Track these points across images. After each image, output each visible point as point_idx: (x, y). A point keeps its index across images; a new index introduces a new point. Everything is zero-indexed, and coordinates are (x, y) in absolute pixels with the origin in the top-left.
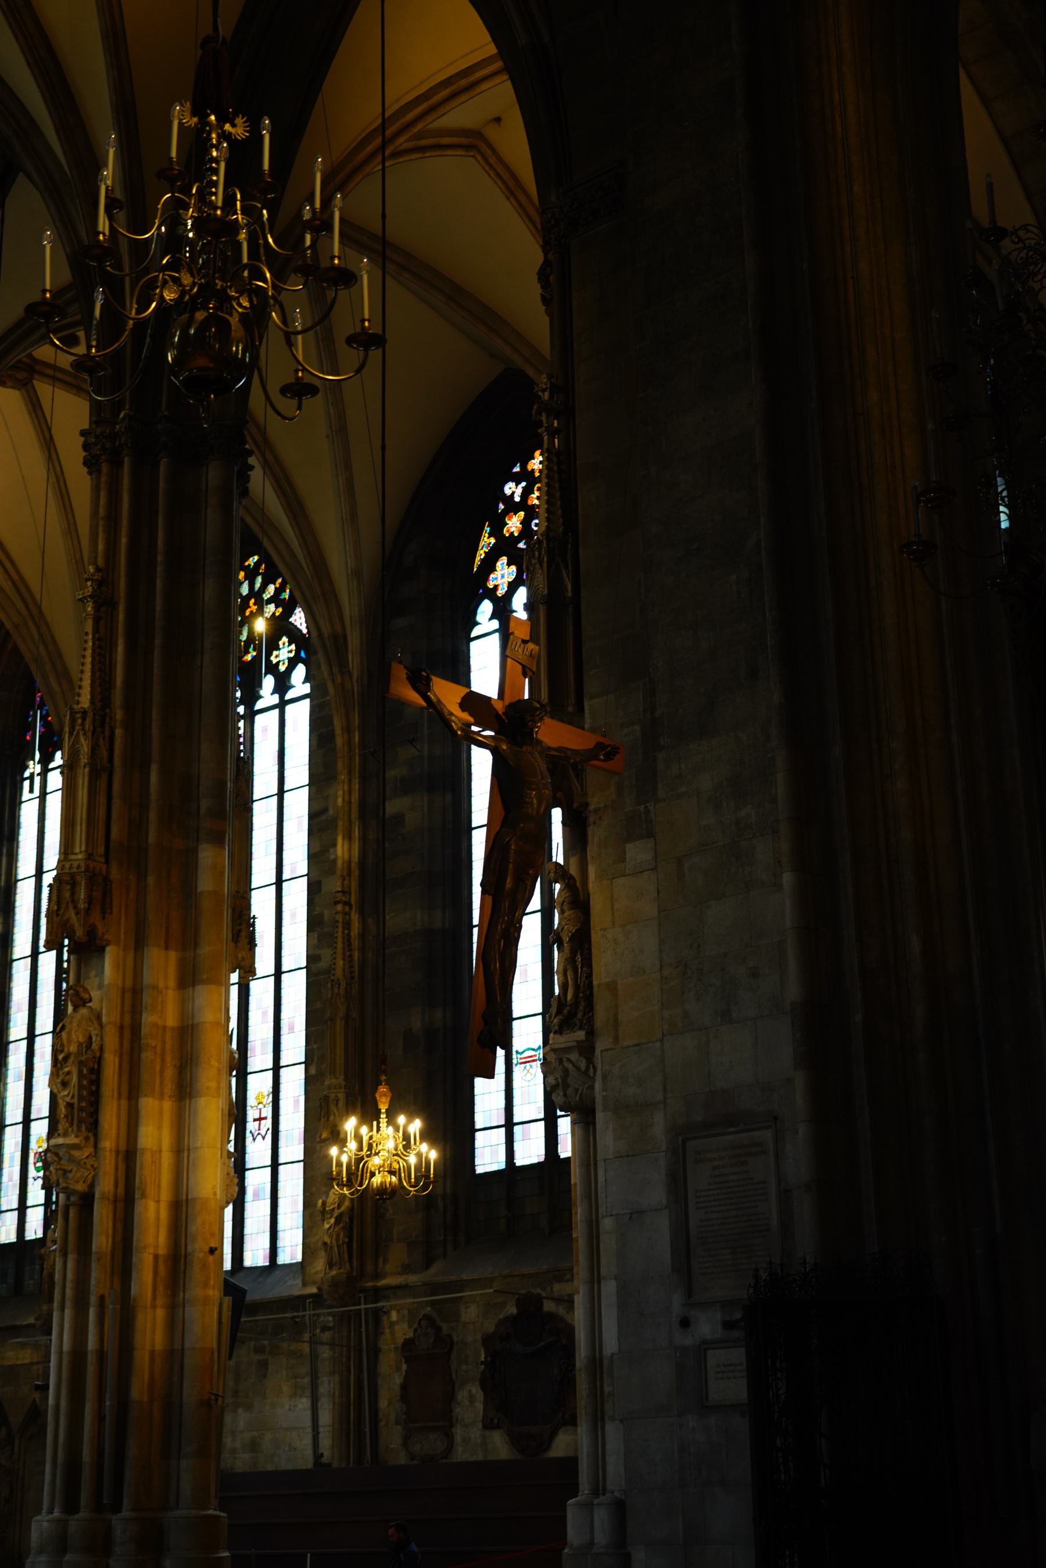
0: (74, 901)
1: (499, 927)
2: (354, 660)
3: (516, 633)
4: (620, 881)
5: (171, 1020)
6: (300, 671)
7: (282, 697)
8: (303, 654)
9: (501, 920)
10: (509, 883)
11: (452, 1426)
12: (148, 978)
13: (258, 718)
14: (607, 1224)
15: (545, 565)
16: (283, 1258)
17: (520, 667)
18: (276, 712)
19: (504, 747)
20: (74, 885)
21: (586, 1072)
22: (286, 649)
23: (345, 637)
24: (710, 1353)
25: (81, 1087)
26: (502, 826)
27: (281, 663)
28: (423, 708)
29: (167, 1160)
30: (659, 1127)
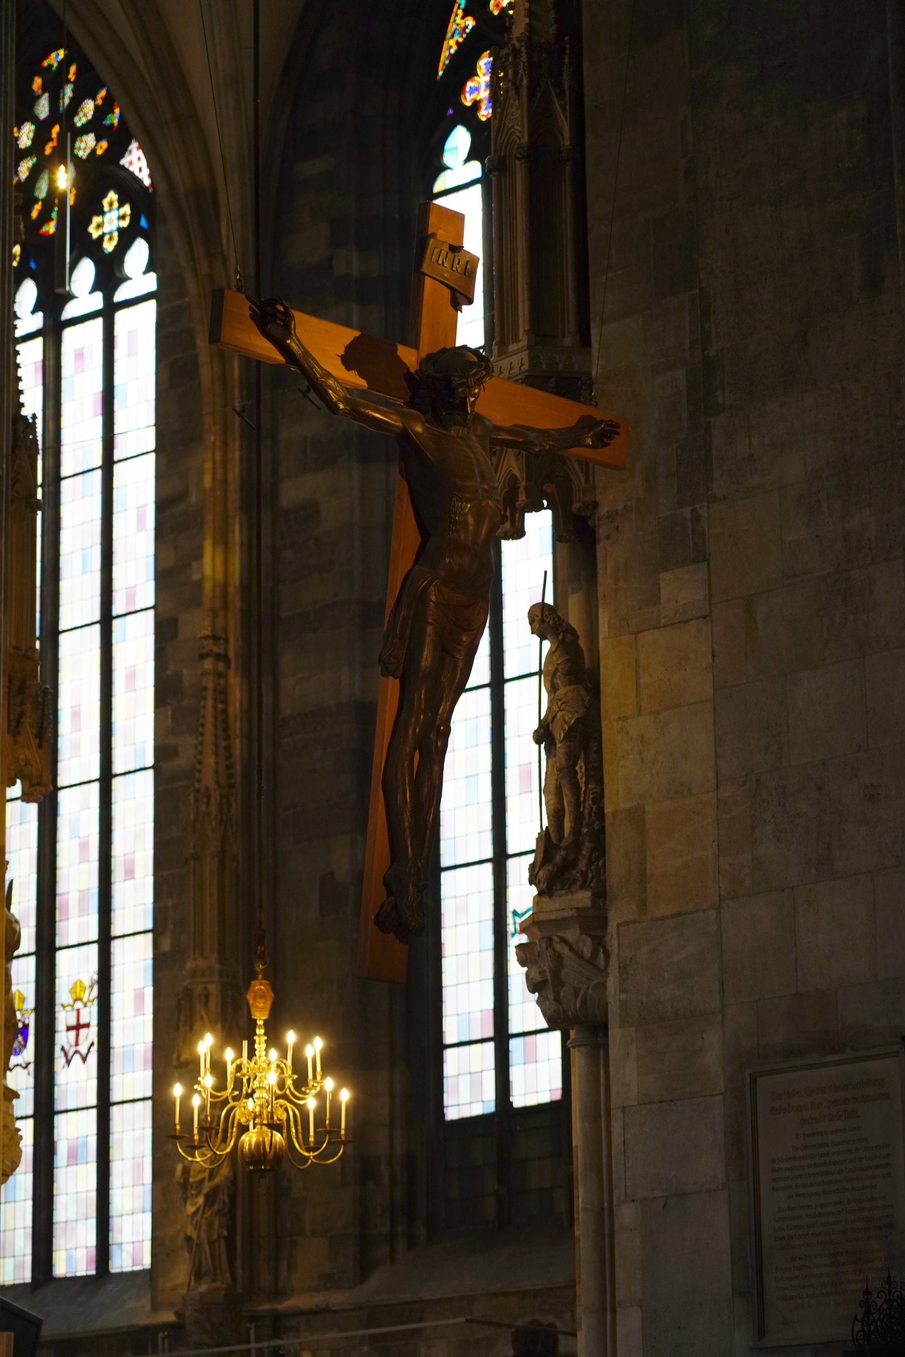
1: (411, 732)
3: (441, 234)
4: (650, 636)
6: (139, 254)
7: (108, 298)
8: (143, 223)
9: (413, 720)
10: (427, 657)
13: (69, 334)
14: (626, 1214)
15: (524, 93)
16: (121, 1262)
17: (447, 292)
18: (99, 322)
19: (419, 429)
21: (592, 961)
22: (114, 215)
23: (214, 192)
26: (416, 561)
27: (106, 238)
28: (277, 367)
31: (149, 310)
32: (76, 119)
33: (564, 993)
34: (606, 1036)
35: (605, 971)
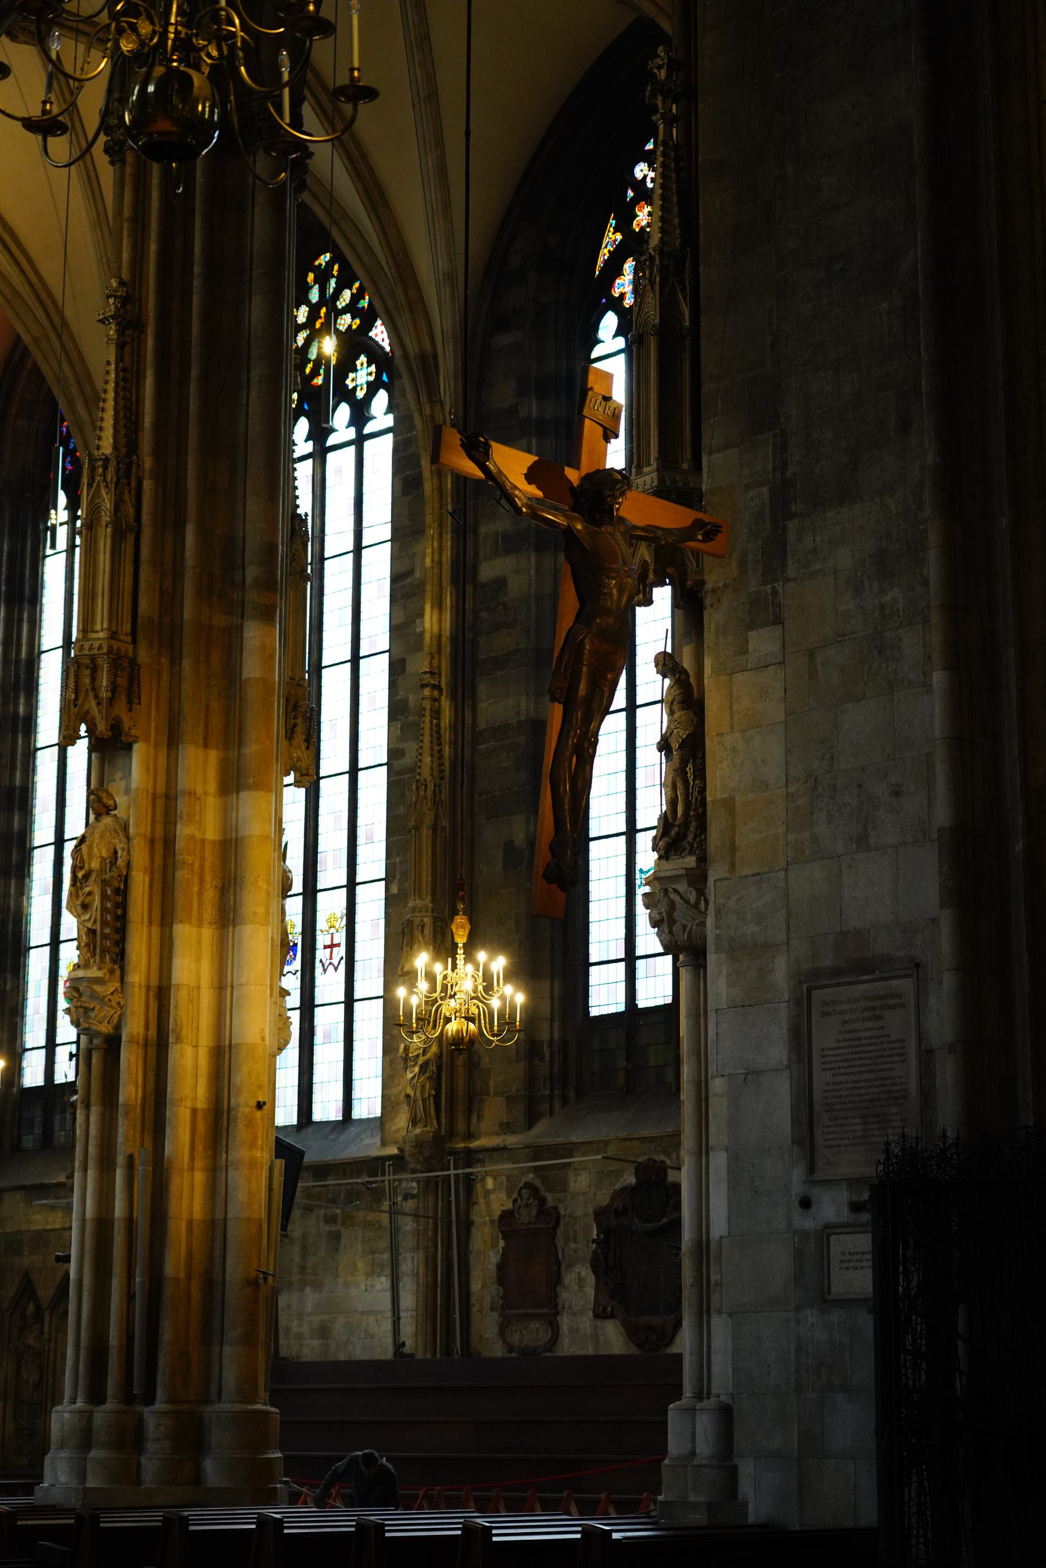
1: (570, 742)
2: (447, 386)
3: (597, 388)
4: (739, 677)
5: (211, 832)
6: (381, 399)
8: (385, 378)
9: (572, 733)
10: (582, 689)
11: (557, 1314)
12: (184, 781)
13: (331, 457)
14: (717, 1085)
15: (657, 287)
17: (601, 429)
18: (352, 449)
19: (579, 527)
20: (94, 669)
21: (696, 906)
23: (435, 357)
24: (833, 1239)
25: (104, 910)
26: (575, 623)
27: (359, 388)
28: (478, 481)
29: (206, 998)
31: (388, 439)
32: (338, 303)
35: (704, 913)
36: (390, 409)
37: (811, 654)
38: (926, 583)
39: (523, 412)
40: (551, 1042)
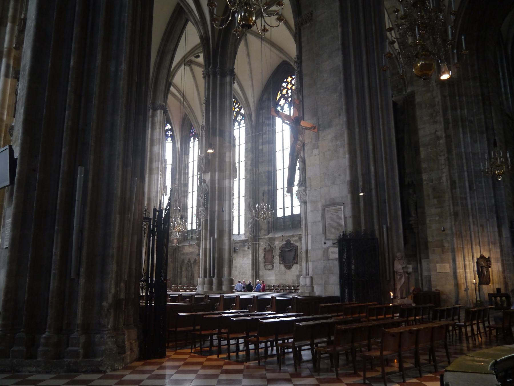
0: (203, 163)
2: (254, 119)
6: (243, 121)
7: (239, 126)
8: (243, 118)
11: (273, 264)
14: (309, 224)
15: (296, 94)
20: (203, 159)
21: (305, 195)
23: (252, 114)
24: (330, 249)
30: (320, 206)
33: (302, 199)
34: (306, 204)
35: (306, 196)
36: (244, 123)
37: (324, 153)
38: (344, 140)
39: (265, 123)
40: (272, 221)
